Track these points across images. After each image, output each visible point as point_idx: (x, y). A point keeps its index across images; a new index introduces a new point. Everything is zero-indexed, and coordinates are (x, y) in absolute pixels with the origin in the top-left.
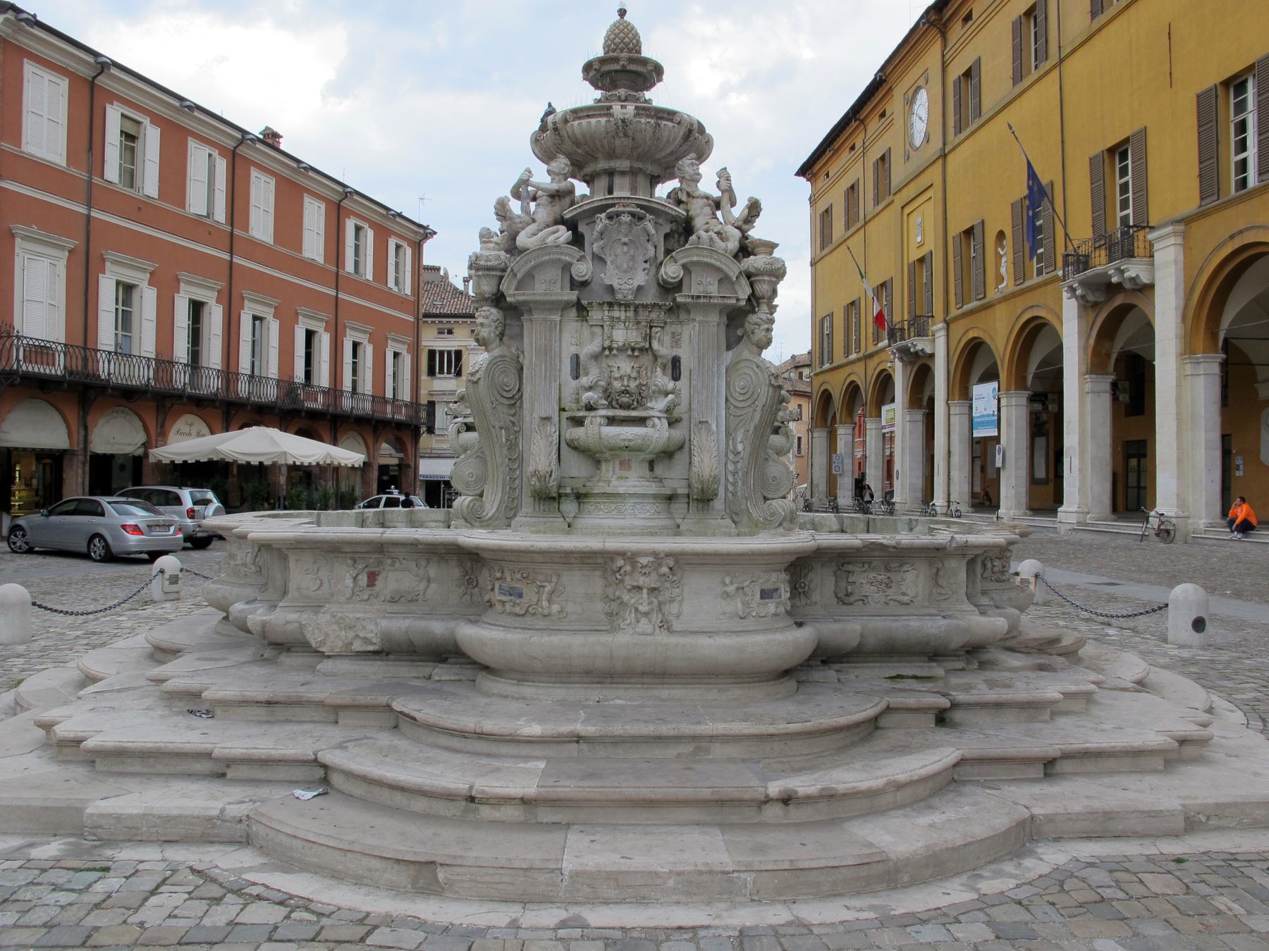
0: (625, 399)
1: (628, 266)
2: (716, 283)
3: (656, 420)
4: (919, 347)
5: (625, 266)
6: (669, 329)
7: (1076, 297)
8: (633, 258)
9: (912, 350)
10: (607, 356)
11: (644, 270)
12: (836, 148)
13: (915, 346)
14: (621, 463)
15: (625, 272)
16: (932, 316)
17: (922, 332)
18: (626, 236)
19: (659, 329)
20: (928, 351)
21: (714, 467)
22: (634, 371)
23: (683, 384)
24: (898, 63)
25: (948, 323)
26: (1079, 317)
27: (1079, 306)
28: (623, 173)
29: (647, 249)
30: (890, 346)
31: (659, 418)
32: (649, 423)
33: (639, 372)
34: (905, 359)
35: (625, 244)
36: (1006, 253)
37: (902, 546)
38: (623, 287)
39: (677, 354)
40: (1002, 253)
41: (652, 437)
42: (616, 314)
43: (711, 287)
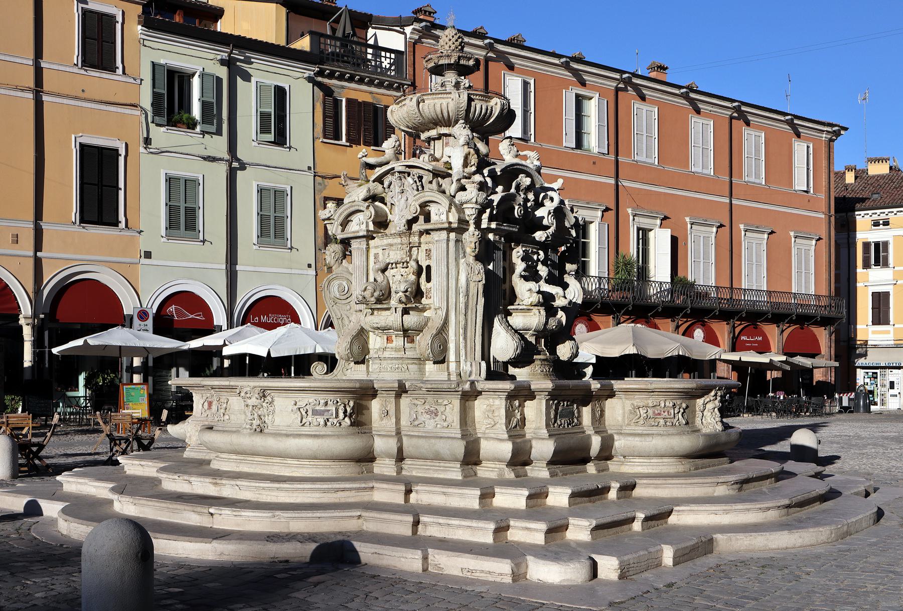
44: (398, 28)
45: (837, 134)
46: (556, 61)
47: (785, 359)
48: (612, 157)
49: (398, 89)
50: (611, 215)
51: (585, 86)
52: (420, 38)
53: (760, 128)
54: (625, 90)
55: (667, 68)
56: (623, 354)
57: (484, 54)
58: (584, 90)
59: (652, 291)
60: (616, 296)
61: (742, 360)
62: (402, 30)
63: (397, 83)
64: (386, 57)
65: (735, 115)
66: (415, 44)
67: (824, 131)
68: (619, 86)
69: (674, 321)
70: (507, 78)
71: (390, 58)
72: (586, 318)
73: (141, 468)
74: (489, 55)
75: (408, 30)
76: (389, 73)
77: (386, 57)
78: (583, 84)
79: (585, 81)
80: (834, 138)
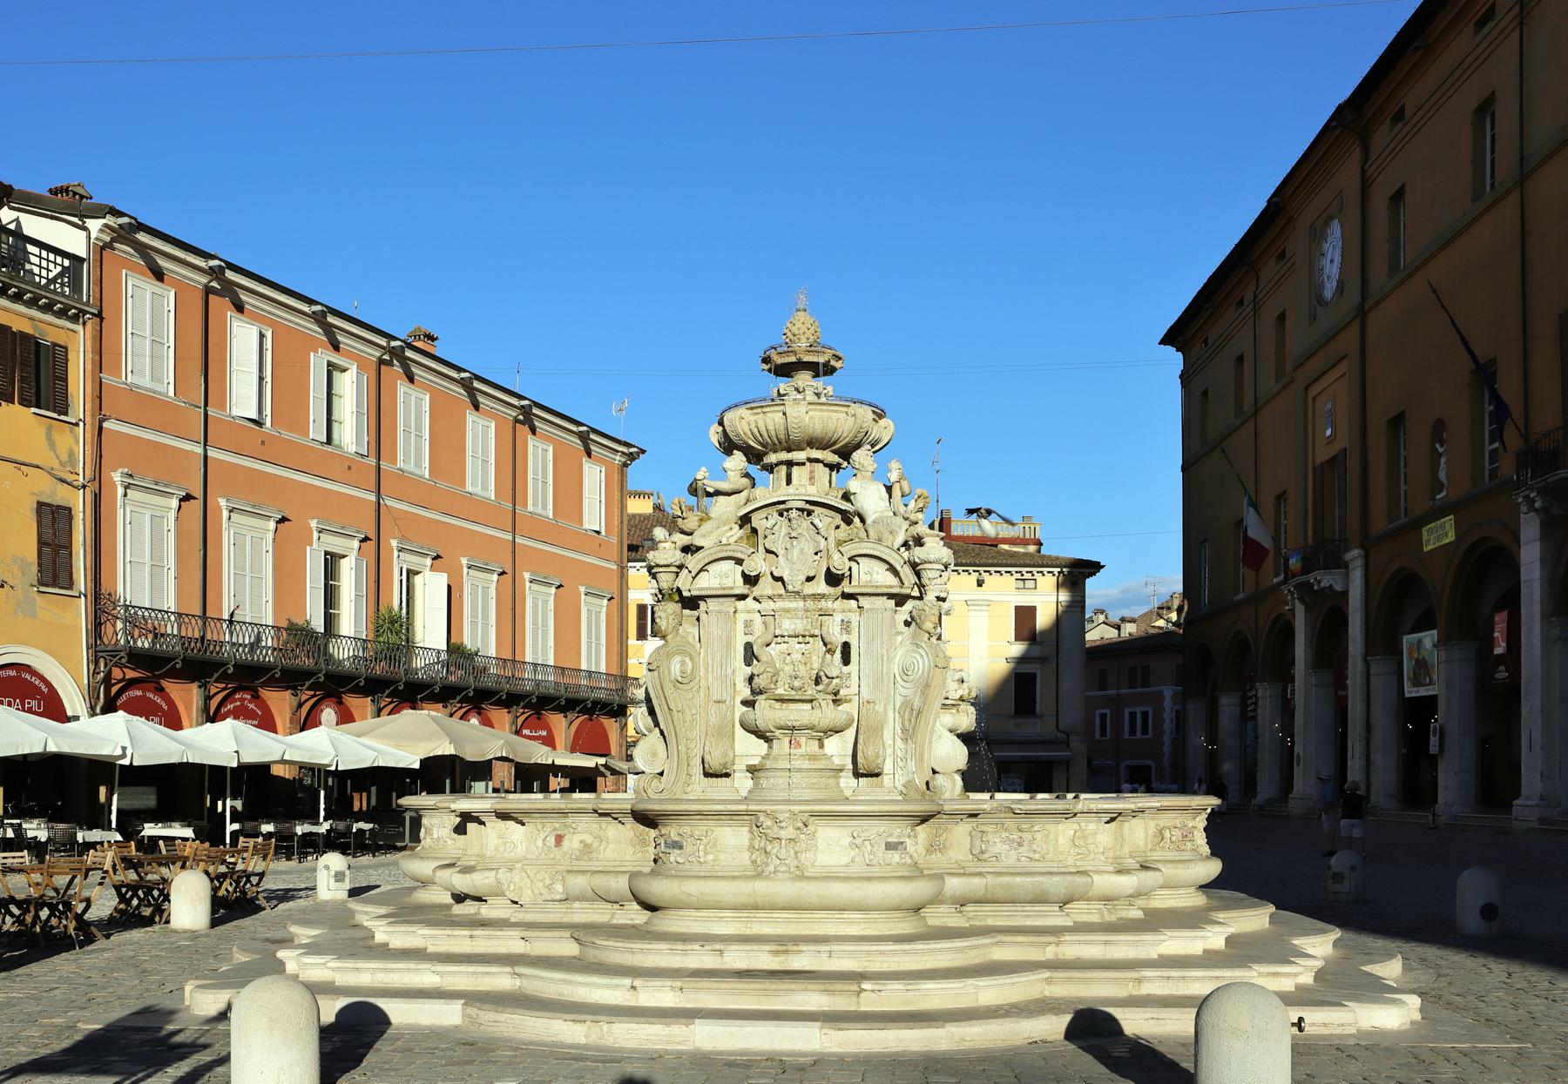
4: (1325, 584)
7: (1536, 511)
9: (1315, 588)
12: (1217, 303)
13: (1319, 582)
16: (1347, 540)
17: (1336, 562)
20: (1338, 588)
24: (1307, 176)
25: (1366, 546)
26: (1542, 538)
27: (1542, 523)
30: (1285, 581)
34: (1307, 600)
36: (1446, 451)
40: (1440, 450)
44: (75, 220)
45: (632, 457)
46: (305, 308)
47: (604, 763)
48: (372, 461)
49: (75, 319)
50: (371, 545)
51: (339, 351)
52: (113, 240)
53: (548, 439)
54: (389, 363)
55: (436, 339)
56: (431, 755)
57: (206, 281)
58: (337, 356)
59: (418, 663)
60: (380, 669)
61: (556, 763)
62: (80, 223)
63: (75, 308)
64: (55, 263)
65: (521, 417)
66: (102, 248)
67: (618, 452)
68: (384, 357)
69: (447, 707)
70: (235, 324)
71: (62, 265)
72: (336, 700)
73: (468, 942)
74: (211, 284)
75: (94, 225)
76: (52, 287)
77: (55, 263)
78: (336, 347)
79: (339, 343)
80: (629, 462)
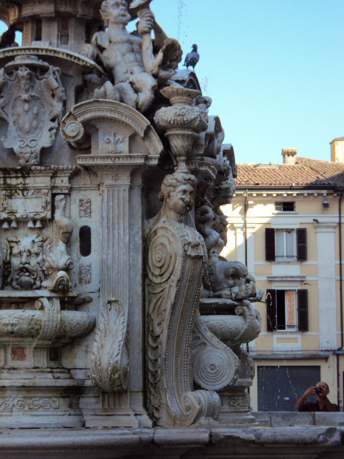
0: (25, 278)
1: (31, 125)
2: (127, 140)
3: (45, 302)
5: (27, 126)
6: (76, 196)
8: (36, 116)
10: (6, 230)
11: (51, 129)
14: (14, 352)
15: (28, 133)
18: (27, 91)
19: (62, 196)
21: (116, 353)
22: (36, 245)
23: (93, 259)
28: (50, 19)
29: (52, 106)
31: (49, 299)
32: (38, 304)
33: (42, 246)
35: (26, 101)
37: (262, 440)
38: (24, 151)
39: (87, 224)
41: (41, 321)
42: (13, 182)
43: (122, 145)
